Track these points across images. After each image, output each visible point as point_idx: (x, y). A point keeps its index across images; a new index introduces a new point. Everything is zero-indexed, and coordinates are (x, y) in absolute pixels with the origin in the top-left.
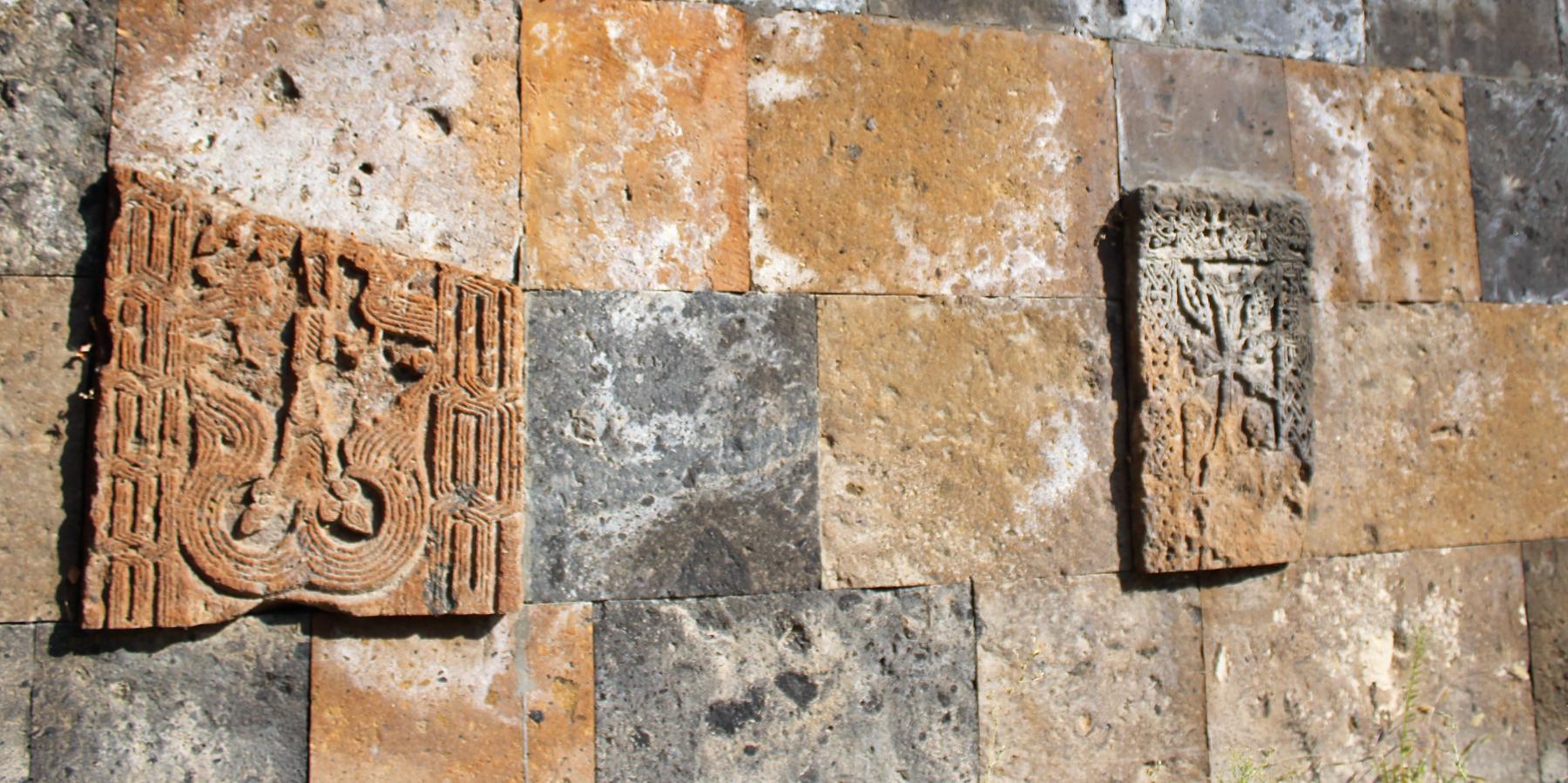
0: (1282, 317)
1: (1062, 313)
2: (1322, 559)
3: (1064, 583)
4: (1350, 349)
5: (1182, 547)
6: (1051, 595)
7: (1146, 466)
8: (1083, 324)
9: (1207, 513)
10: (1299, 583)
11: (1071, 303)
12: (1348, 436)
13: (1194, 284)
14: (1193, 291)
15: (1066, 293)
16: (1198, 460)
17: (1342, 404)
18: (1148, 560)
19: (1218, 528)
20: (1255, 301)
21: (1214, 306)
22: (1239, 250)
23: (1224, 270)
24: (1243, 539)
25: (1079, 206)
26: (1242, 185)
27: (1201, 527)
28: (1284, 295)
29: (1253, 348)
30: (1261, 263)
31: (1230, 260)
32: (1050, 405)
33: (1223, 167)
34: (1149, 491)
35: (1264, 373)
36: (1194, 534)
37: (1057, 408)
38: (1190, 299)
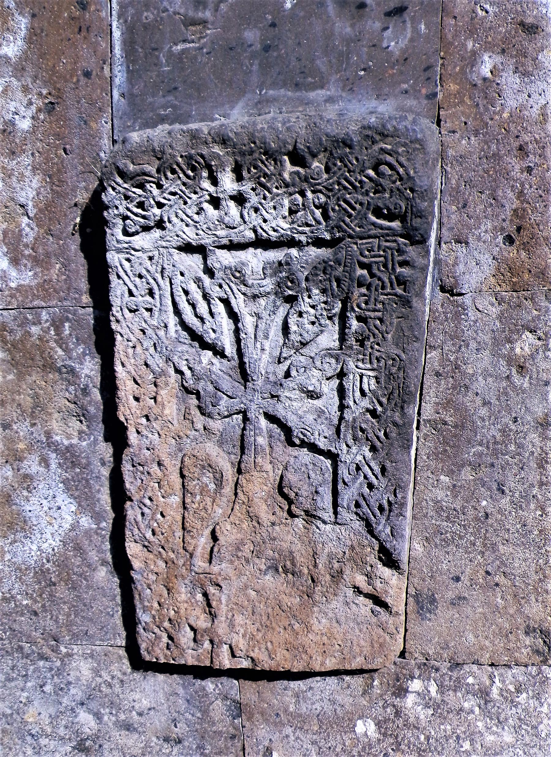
0: (354, 324)
1: (35, 330)
2: (444, 667)
3: (55, 650)
4: (521, 368)
5: (186, 637)
6: (41, 663)
7: (128, 533)
8: (61, 342)
9: (222, 601)
10: (402, 692)
11: (44, 315)
12: (505, 502)
13: (198, 281)
14: (197, 295)
15: (36, 303)
16: (207, 532)
17: (496, 453)
18: (143, 646)
19: (239, 619)
20: (304, 305)
21: (233, 316)
22: (278, 224)
23: (254, 260)
24: (281, 636)
25: (54, 176)
26: (282, 118)
27: (213, 616)
28: (357, 292)
29: (297, 377)
30: (318, 243)
31: (262, 243)
32: (21, 446)
33: (297, 86)
34: (136, 564)
35: (320, 413)
36: (203, 622)
37: (30, 448)
38: (194, 306)
